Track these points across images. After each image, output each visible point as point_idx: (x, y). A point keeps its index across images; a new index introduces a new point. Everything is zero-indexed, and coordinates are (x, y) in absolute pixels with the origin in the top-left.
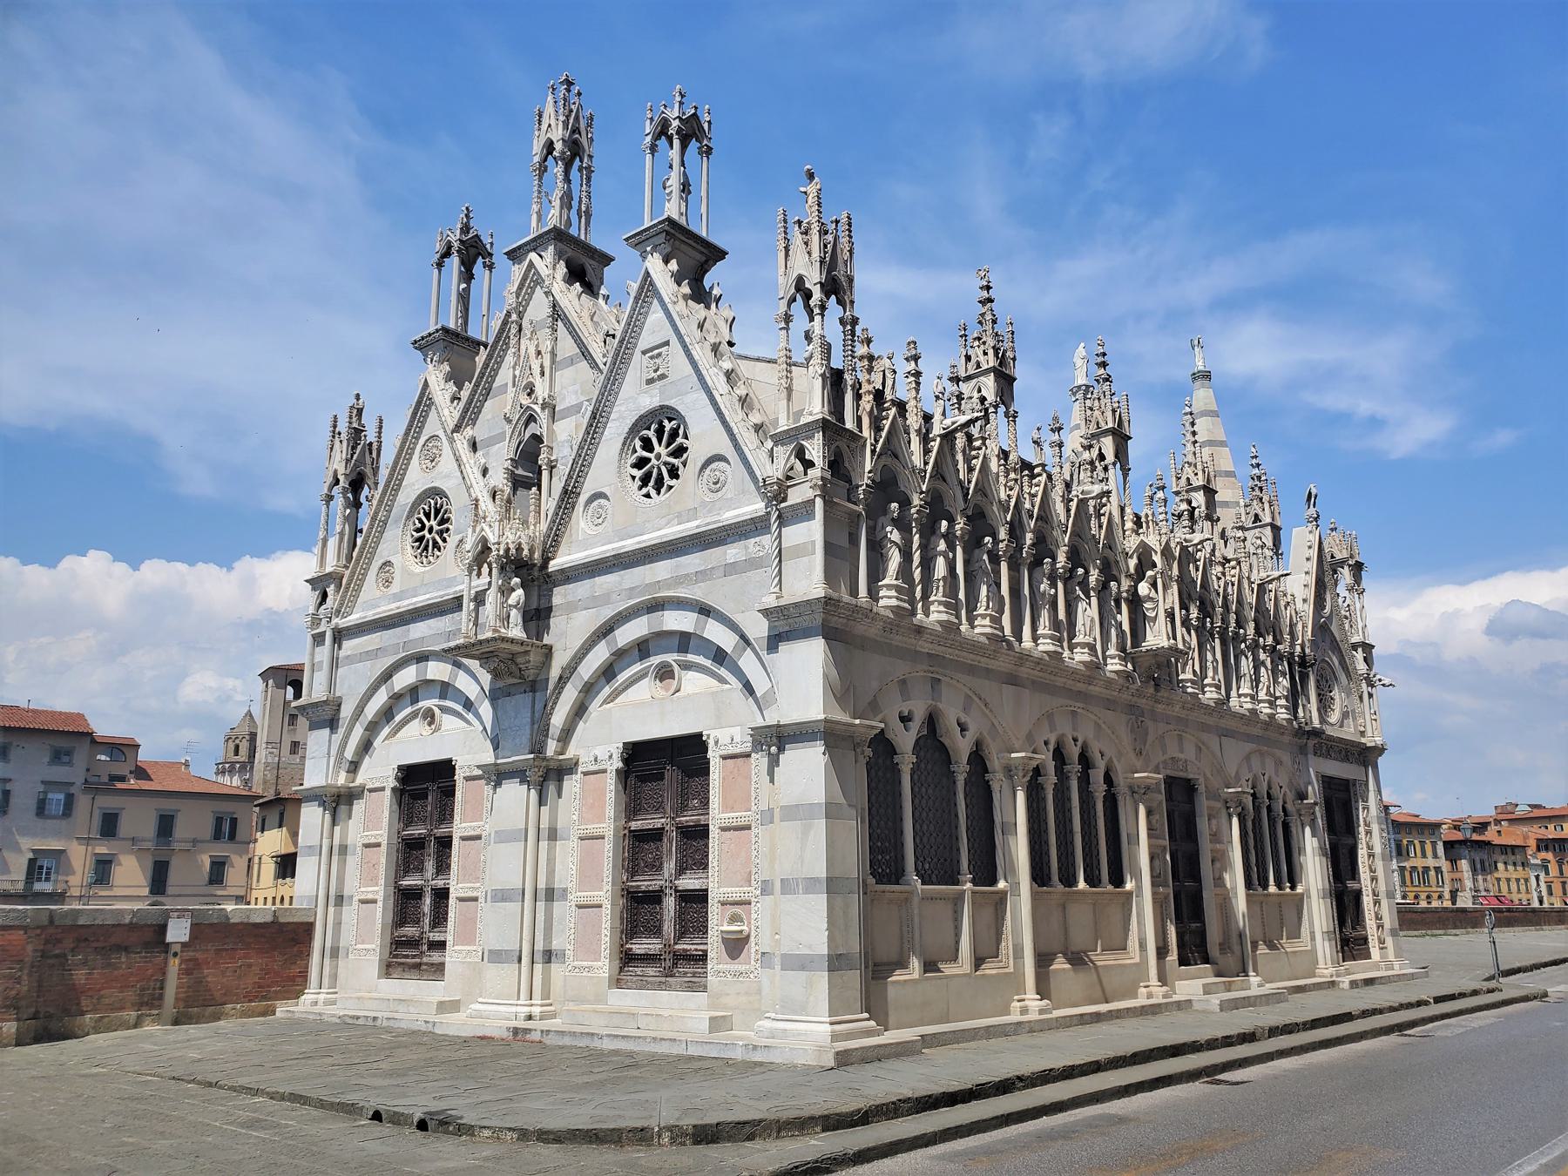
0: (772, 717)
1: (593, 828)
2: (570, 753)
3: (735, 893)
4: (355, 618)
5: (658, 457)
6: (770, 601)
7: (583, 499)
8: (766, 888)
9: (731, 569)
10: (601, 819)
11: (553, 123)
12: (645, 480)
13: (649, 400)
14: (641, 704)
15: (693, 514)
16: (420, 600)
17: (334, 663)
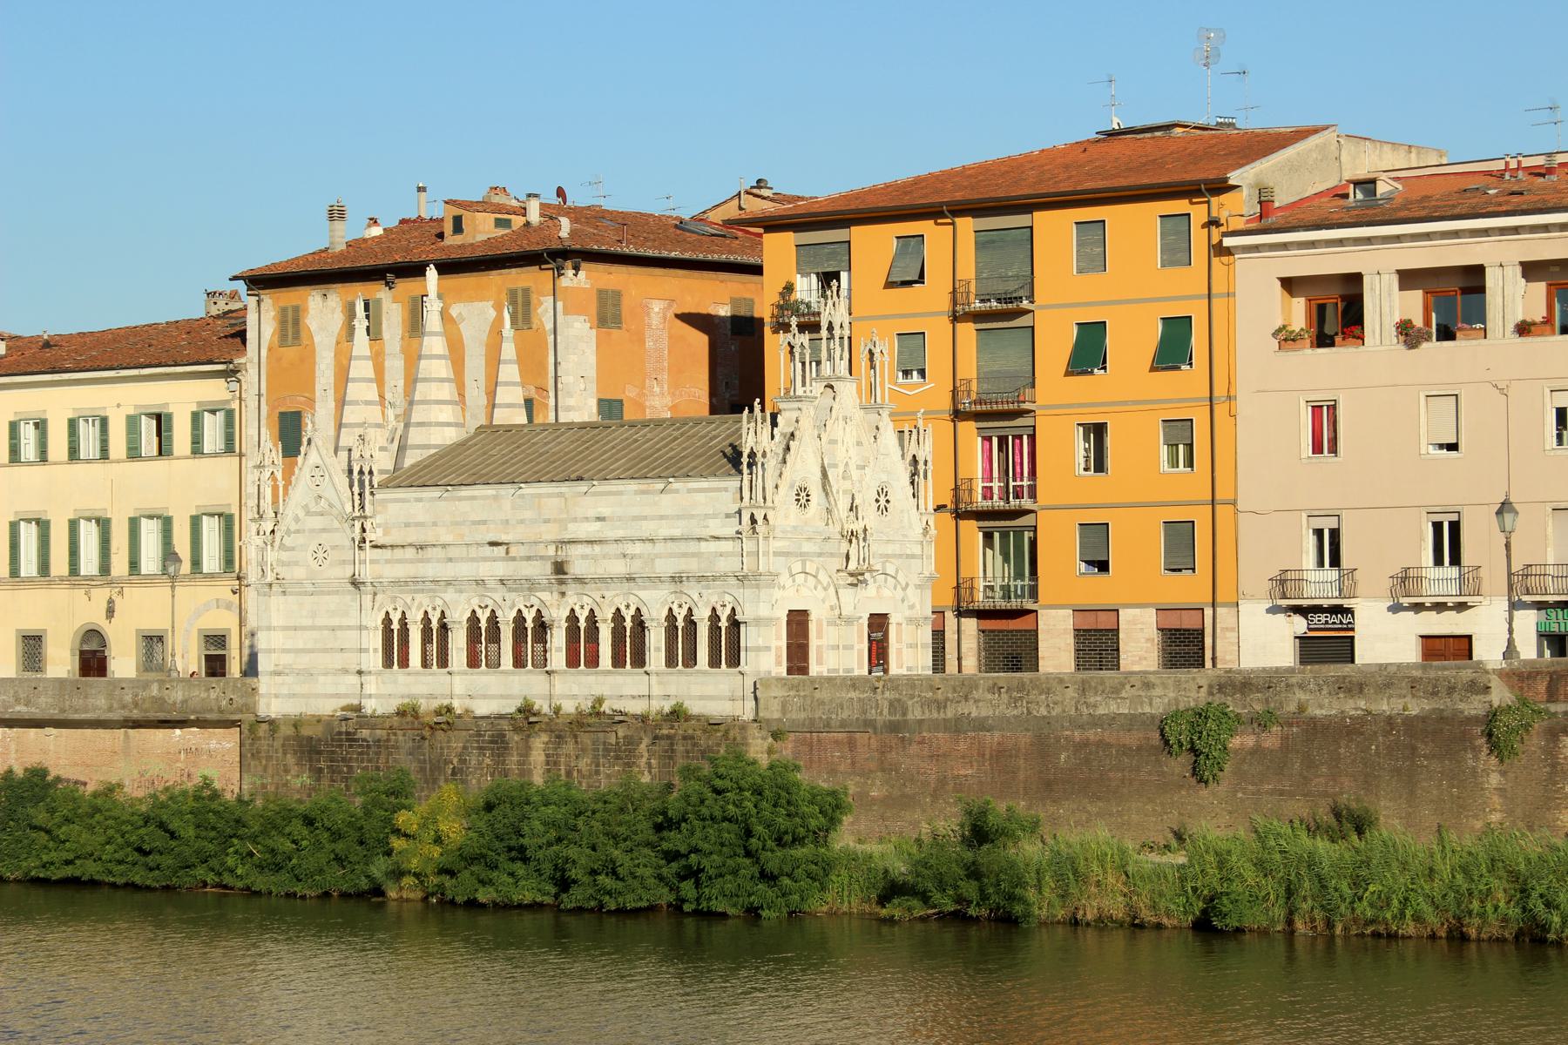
9: (908, 557)
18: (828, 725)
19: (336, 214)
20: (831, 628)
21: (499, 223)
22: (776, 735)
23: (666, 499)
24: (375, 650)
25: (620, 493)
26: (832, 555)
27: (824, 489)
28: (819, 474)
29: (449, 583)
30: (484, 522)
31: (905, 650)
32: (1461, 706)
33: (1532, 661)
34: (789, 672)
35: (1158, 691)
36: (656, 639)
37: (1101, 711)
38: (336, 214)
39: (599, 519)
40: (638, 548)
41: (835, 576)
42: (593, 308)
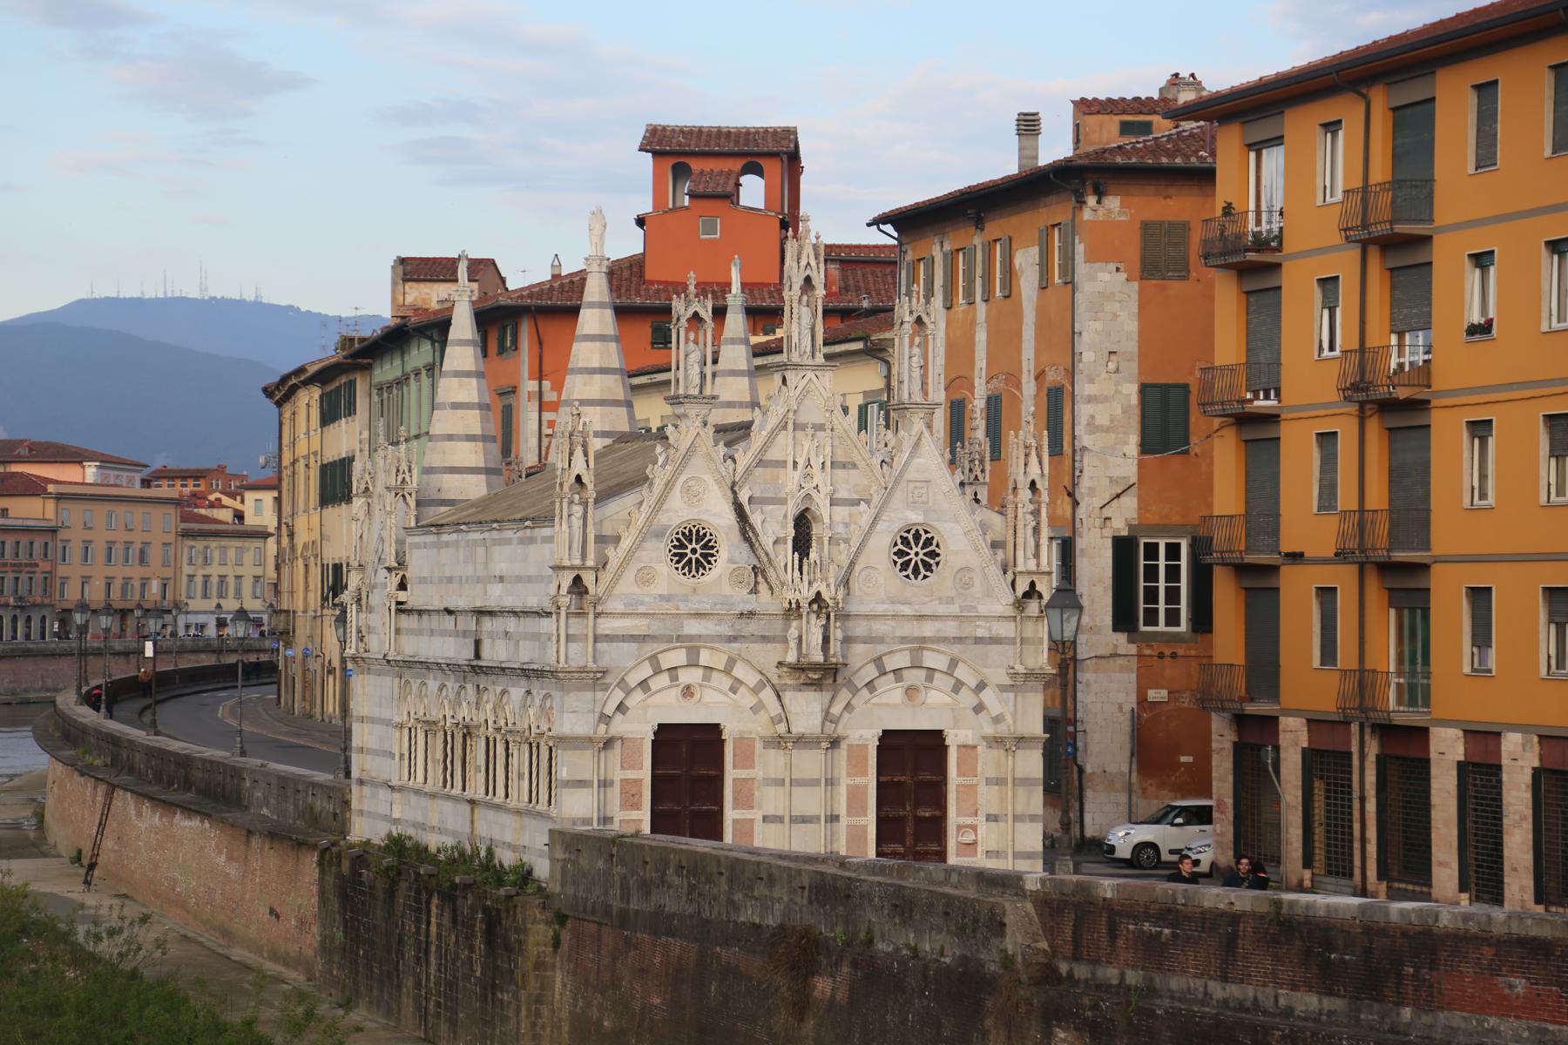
0: (1003, 730)
1: (859, 780)
2: (840, 731)
3: (969, 821)
4: (618, 606)
5: (917, 554)
6: (1020, 669)
7: (857, 568)
8: (991, 818)
9: (979, 640)
10: (864, 773)
11: (813, 263)
12: (905, 566)
13: (915, 517)
14: (895, 706)
15: (950, 601)
16: (694, 606)
17: (596, 639)
18: (585, 911)
19: (1028, 125)
20: (772, 752)
21: (1126, 128)
22: (562, 919)
23: (532, 548)
24: (402, 755)
25: (508, 542)
26: (765, 639)
27: (747, 539)
28: (730, 517)
29: (426, 665)
30: (450, 580)
31: (982, 789)
32: (984, 955)
33: (829, 886)
34: (660, 822)
35: (777, 892)
36: (520, 759)
37: (742, 919)
38: (1028, 125)
39: (502, 579)
40: (511, 624)
41: (773, 673)
42: (1134, 252)
